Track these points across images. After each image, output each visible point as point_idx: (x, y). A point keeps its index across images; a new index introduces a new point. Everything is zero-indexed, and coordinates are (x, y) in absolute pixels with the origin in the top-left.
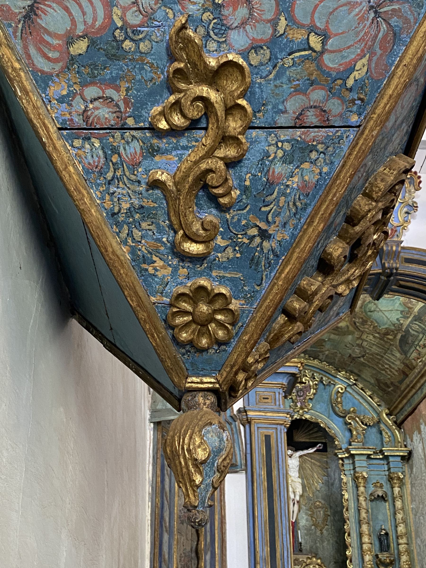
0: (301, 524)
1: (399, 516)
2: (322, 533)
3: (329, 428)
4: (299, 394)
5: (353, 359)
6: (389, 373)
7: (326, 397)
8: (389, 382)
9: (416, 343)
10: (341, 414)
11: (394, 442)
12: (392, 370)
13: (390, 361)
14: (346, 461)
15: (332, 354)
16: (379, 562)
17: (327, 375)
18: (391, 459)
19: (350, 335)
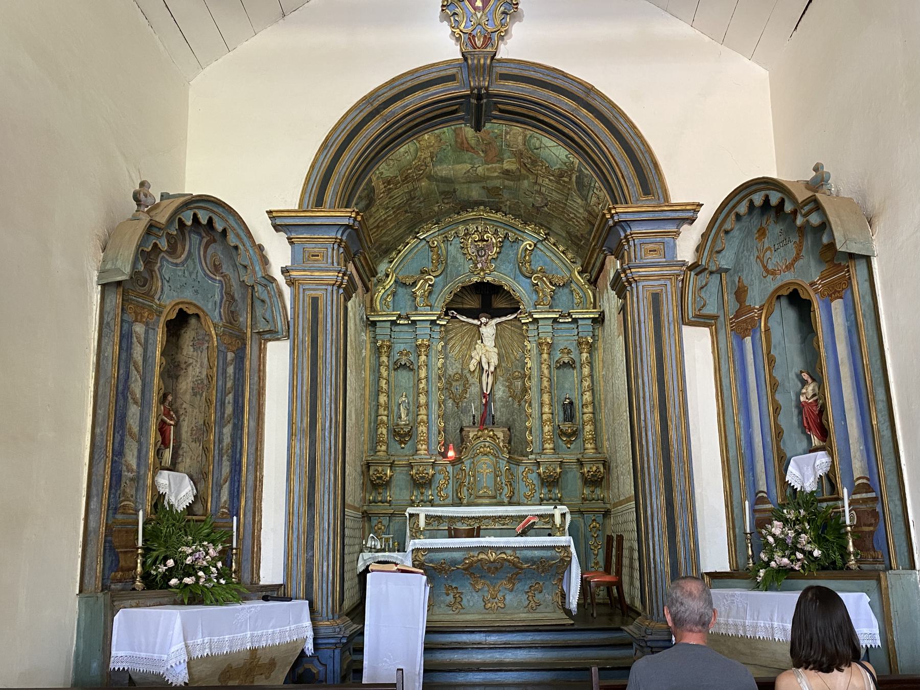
1: (586, 384)
2: (520, 405)
5: (538, 209)
7: (512, 254)
8: (579, 235)
10: (528, 275)
11: (582, 304)
18: (580, 322)
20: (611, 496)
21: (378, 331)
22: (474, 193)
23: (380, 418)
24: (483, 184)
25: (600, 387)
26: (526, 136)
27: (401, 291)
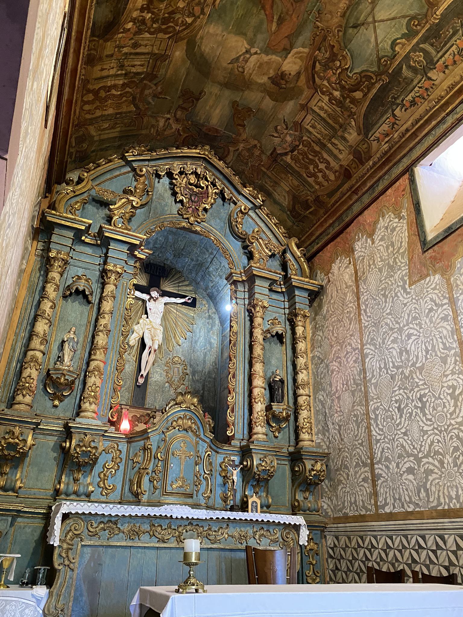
4: (193, 199)
6: (321, 179)
8: (311, 198)
9: (398, 101)
10: (241, 236)
12: (327, 172)
14: (240, 288)
15: (248, 150)
17: (231, 187)
18: (297, 293)
19: (291, 100)
20: (324, 504)
21: (54, 238)
22: (217, 111)
27: (91, 208)
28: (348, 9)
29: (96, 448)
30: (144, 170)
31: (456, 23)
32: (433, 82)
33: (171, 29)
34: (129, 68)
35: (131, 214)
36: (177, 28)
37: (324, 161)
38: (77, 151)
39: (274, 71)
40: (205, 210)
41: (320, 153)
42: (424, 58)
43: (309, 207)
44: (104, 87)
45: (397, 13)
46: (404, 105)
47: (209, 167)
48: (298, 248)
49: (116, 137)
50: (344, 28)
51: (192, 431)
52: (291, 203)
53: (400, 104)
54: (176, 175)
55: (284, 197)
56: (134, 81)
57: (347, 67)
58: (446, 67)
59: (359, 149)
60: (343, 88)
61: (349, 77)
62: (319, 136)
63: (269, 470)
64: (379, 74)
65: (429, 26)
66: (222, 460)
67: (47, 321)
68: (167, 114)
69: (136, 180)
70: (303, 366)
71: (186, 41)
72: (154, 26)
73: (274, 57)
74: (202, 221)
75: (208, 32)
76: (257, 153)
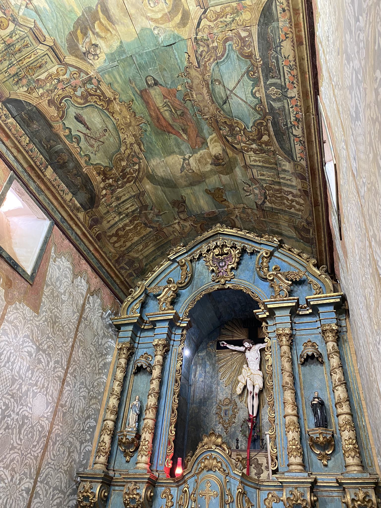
0: (264, 420)
3: (253, 293)
4: (221, 265)
6: (298, 207)
9: (289, 125)
12: (297, 199)
13: (288, 186)
15: (243, 212)
16: (311, 443)
17: (250, 243)
18: (321, 310)
19: (235, 167)
21: (121, 334)
23: (105, 422)
24: (204, 187)
25: (358, 383)
26: (207, 84)
28: (211, 97)
29: (137, 494)
30: (183, 261)
31: (272, 54)
32: (295, 99)
33: (131, 179)
34: (126, 211)
35: (172, 297)
36: (134, 175)
37: (289, 193)
38: (134, 271)
39: (210, 158)
40: (232, 269)
41: (281, 189)
42: (276, 89)
43: (308, 231)
44: (119, 229)
45: (237, 77)
46: (294, 125)
47: (226, 237)
48: (318, 268)
49: (155, 250)
50: (220, 108)
51: (219, 470)
52: (297, 232)
53: (292, 127)
54: (204, 254)
55: (289, 230)
56: (136, 216)
57: (244, 127)
58: (293, 83)
59: (298, 172)
60: (254, 140)
61: (250, 132)
62: (270, 179)
63: (300, 504)
64: (264, 118)
65: (260, 69)
66: (266, 497)
67: (115, 396)
68: (175, 220)
69: (182, 270)
70: (337, 383)
71: (145, 178)
72: (119, 183)
73: (201, 151)
74: (231, 279)
75: (153, 165)
76: (249, 211)
